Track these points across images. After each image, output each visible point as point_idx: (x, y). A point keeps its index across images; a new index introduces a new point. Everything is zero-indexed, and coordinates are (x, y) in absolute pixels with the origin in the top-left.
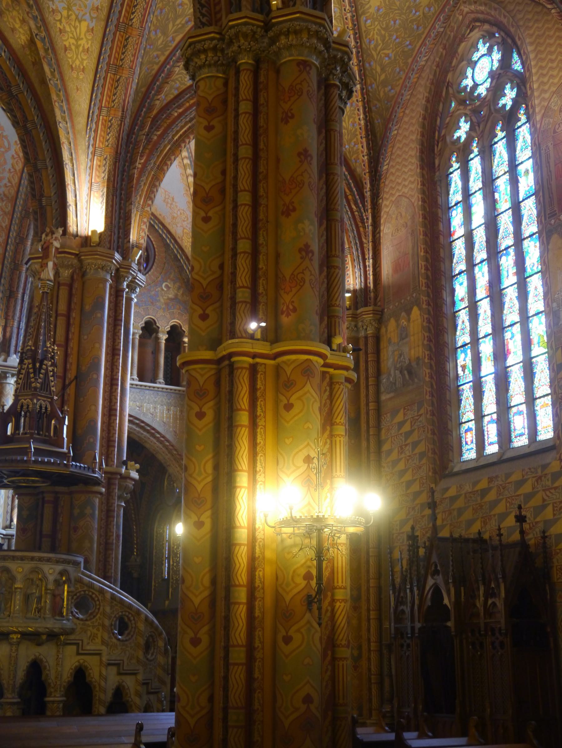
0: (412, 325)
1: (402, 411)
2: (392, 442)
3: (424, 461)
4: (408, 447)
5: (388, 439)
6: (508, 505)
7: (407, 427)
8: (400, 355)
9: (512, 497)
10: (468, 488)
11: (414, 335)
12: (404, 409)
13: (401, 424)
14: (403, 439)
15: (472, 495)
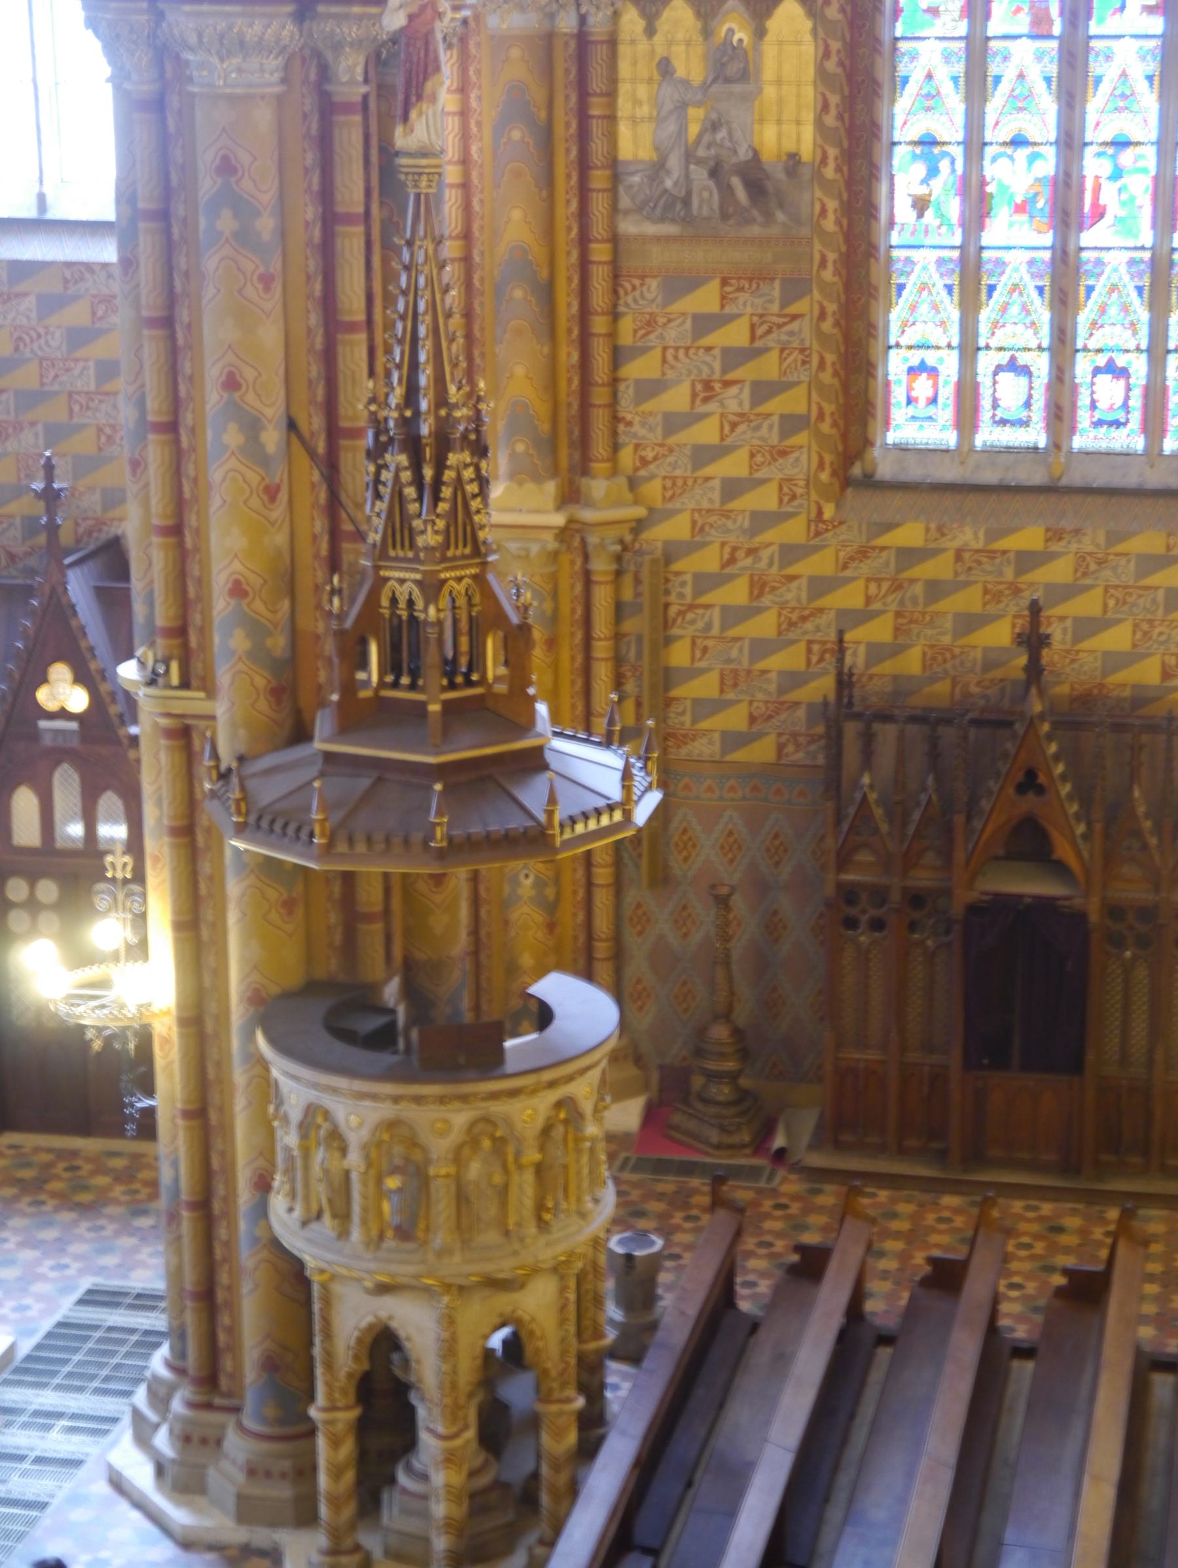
0: (769, 49)
1: (715, 284)
2: (664, 361)
3: (802, 438)
4: (734, 390)
5: (644, 350)
6: (1111, 603)
7: (735, 335)
8: (715, 126)
9: (1126, 587)
10: (968, 536)
11: (779, 82)
12: (725, 282)
13: (705, 324)
14: (717, 365)
15: (984, 560)
